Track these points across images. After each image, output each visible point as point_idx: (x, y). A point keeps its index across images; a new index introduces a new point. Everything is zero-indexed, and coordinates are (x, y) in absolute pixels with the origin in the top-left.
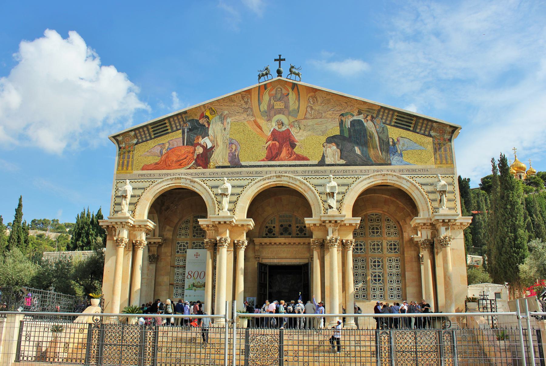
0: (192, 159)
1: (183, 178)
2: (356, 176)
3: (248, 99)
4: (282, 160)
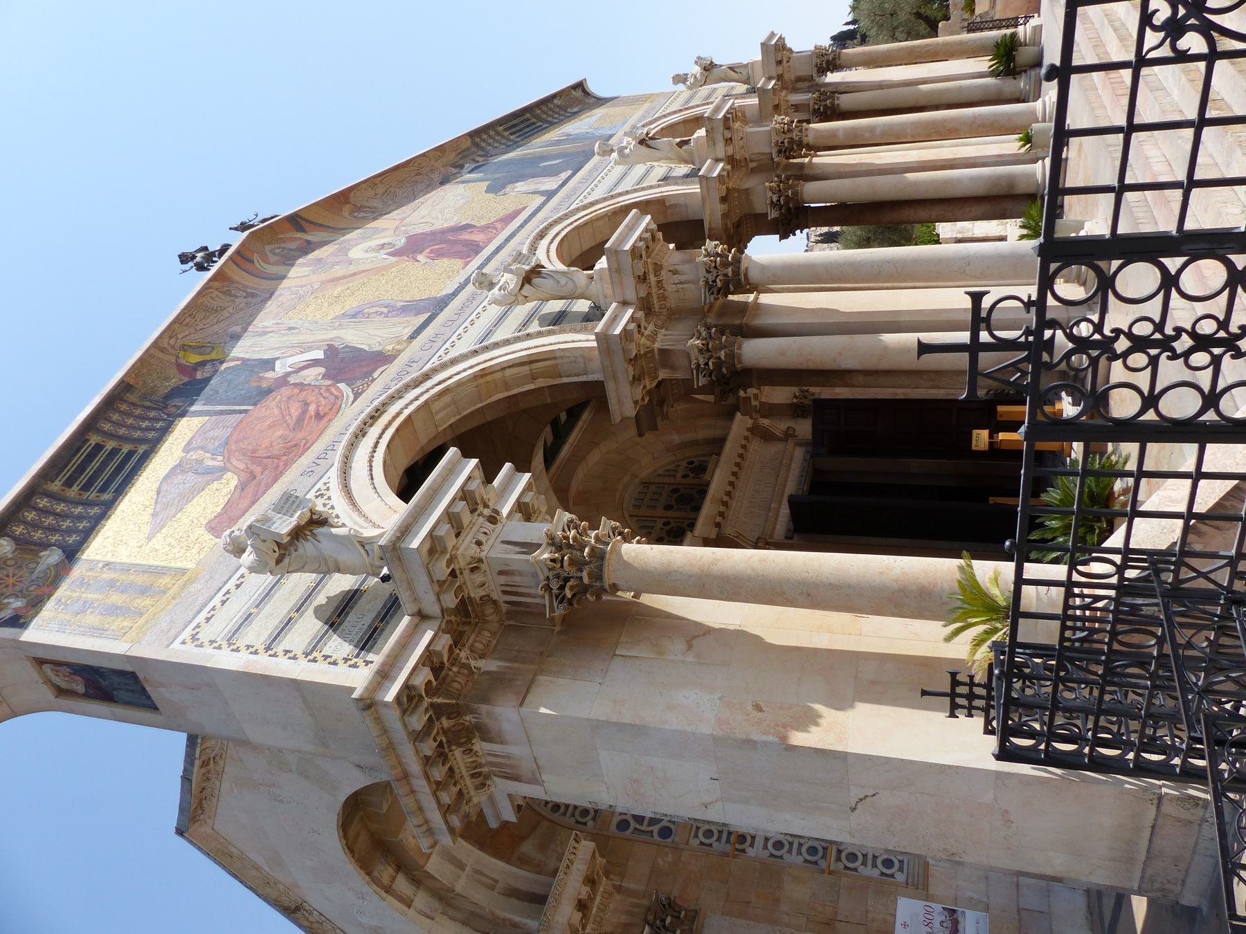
3: (244, 291)
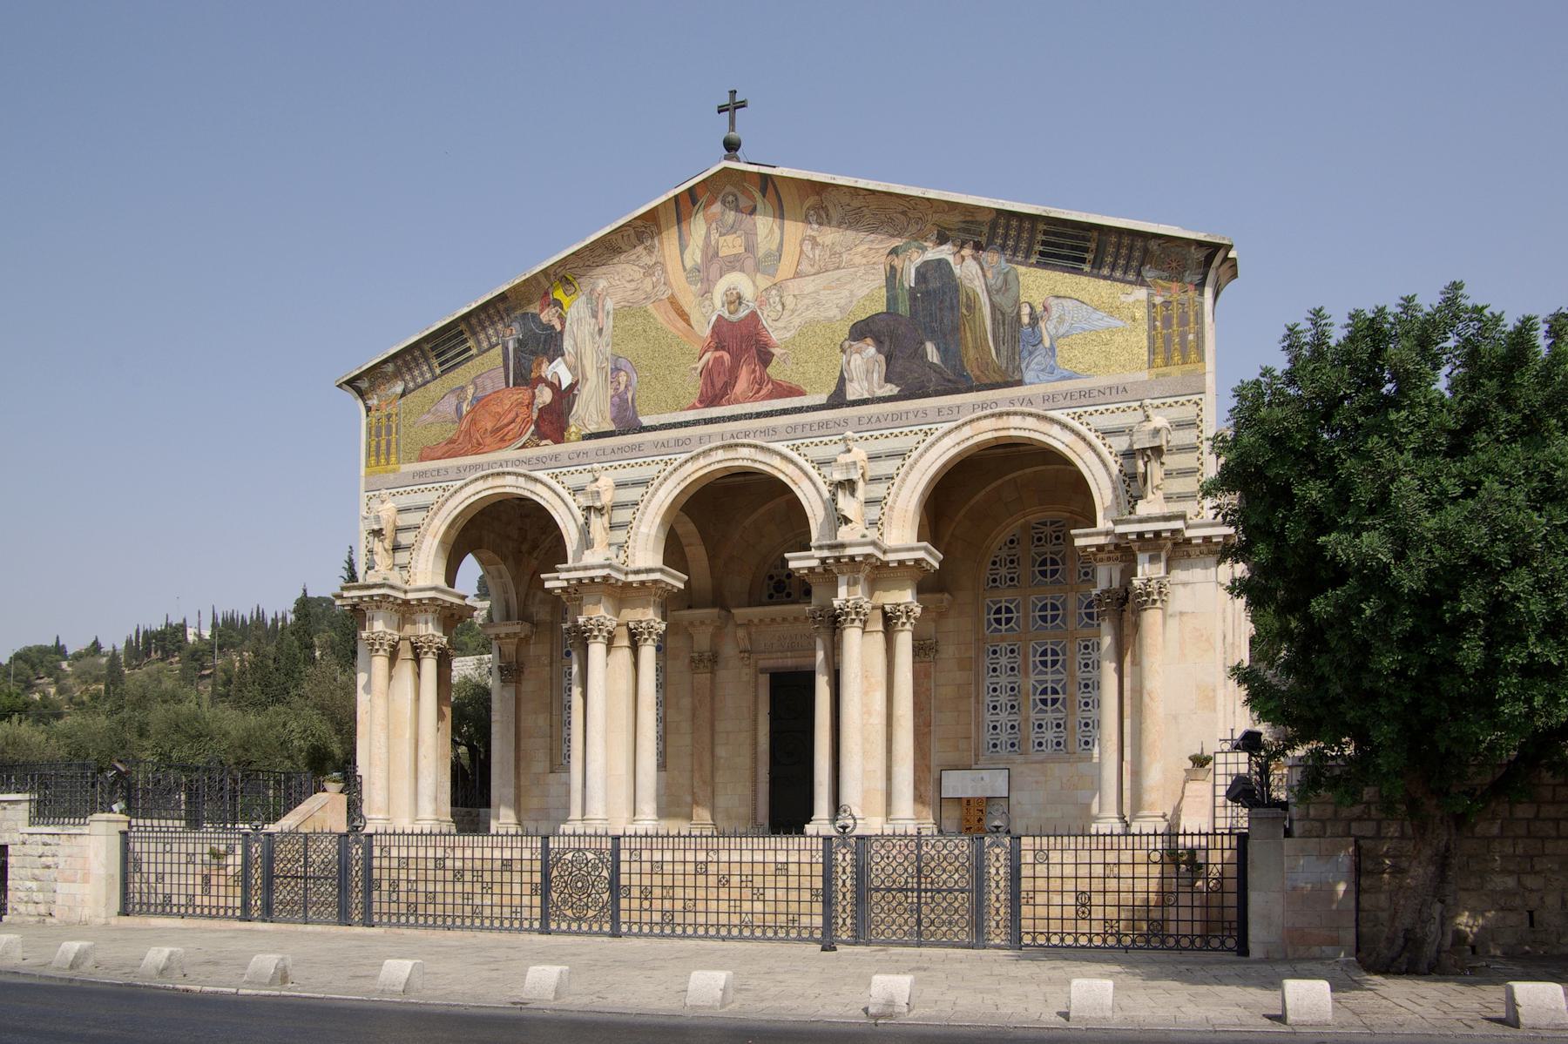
1: (509, 473)
2: (925, 428)
4: (737, 401)
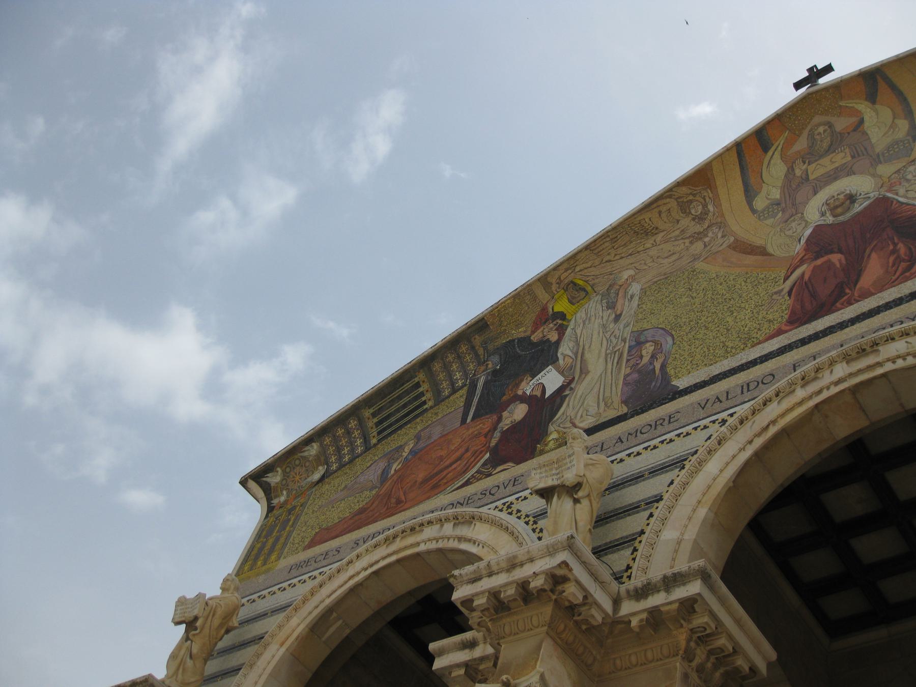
0: (481, 452)
